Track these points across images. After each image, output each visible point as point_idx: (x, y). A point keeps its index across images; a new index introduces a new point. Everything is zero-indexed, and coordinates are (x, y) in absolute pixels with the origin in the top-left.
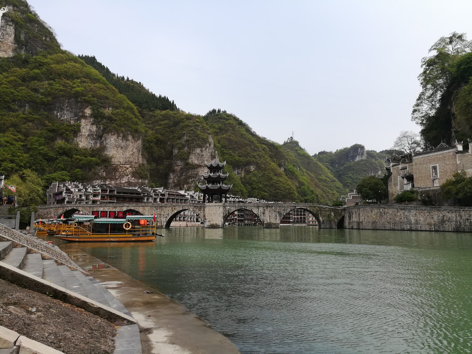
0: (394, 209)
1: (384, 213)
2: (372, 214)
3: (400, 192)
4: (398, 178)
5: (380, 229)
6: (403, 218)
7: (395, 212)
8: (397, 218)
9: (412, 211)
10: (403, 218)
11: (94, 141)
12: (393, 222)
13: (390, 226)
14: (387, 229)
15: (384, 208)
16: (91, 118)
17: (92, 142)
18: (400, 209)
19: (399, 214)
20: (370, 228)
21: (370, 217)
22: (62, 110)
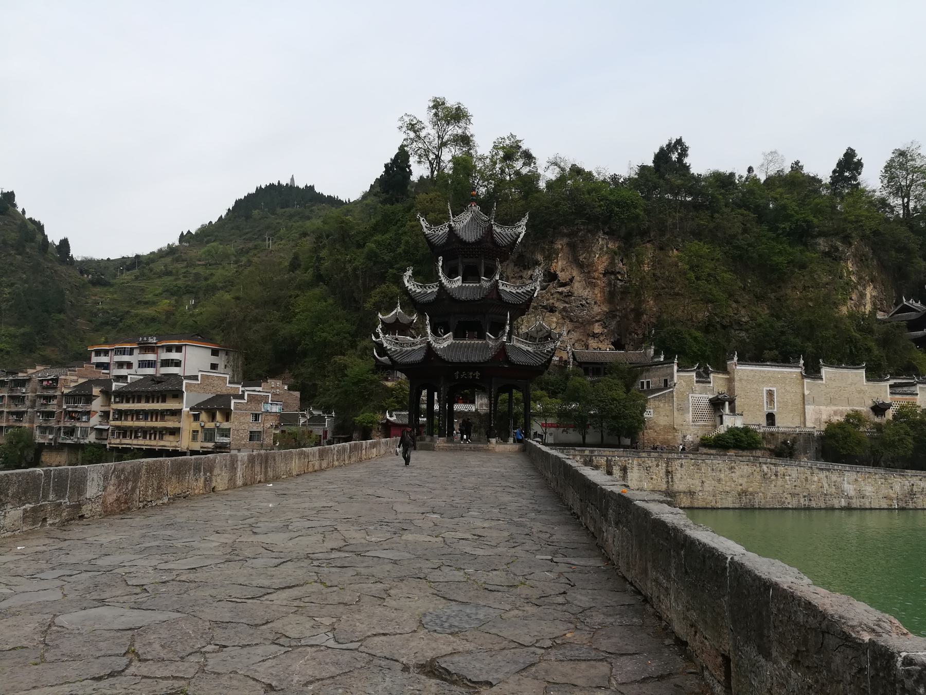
0: (802, 468)
1: (776, 475)
2: (733, 475)
3: (692, 425)
4: (690, 397)
5: (768, 507)
6: (826, 485)
7: (804, 473)
8: (813, 486)
9: (847, 474)
10: (826, 485)
12: (805, 494)
13: (799, 501)
14: (790, 506)
15: (775, 465)
18: (817, 468)
19: (816, 479)
20: (731, 506)
21: (726, 482)
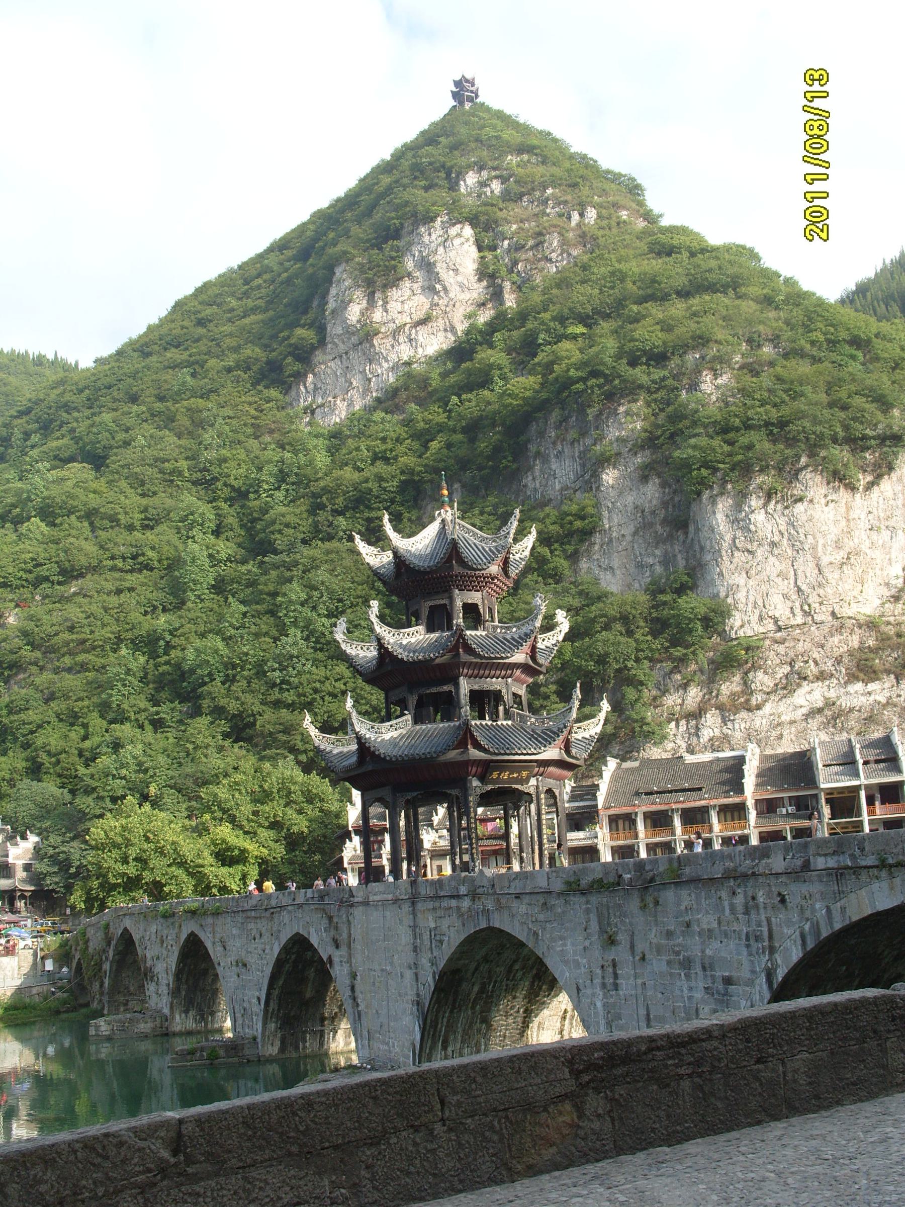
11: (658, 552)
16: (636, 454)
17: (650, 561)
22: (545, 460)
